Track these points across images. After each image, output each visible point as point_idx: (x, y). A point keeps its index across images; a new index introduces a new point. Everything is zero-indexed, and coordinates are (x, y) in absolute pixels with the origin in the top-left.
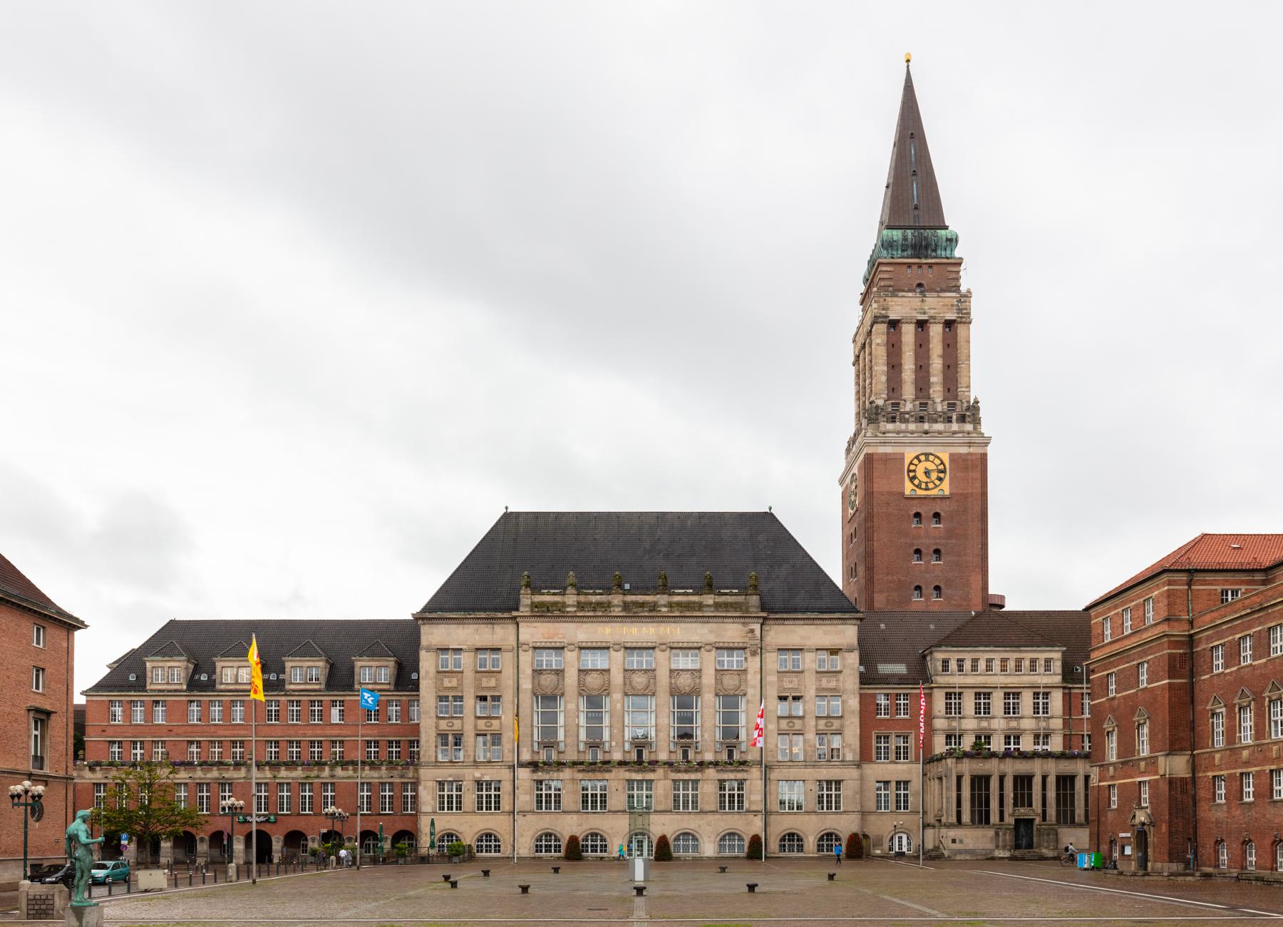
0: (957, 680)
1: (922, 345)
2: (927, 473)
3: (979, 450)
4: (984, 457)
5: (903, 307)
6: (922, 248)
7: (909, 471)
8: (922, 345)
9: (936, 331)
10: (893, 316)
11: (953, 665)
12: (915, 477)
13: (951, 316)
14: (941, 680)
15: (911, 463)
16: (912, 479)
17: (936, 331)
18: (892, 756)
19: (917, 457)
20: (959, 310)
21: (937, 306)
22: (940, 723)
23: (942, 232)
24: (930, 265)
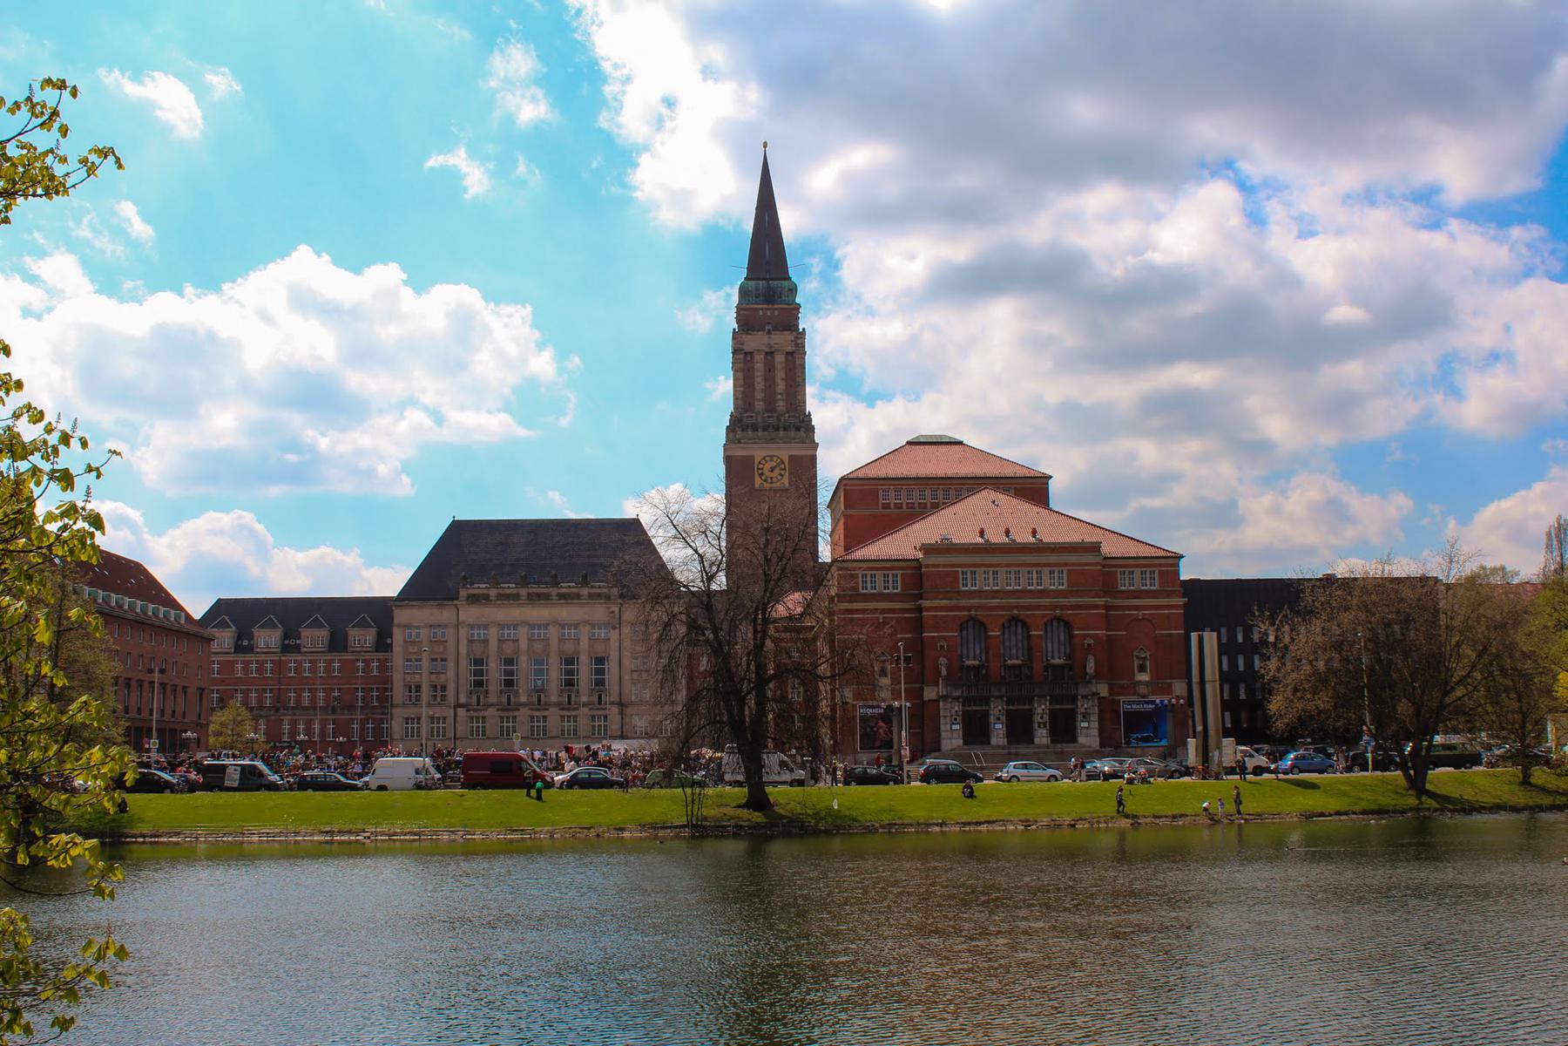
1: (770, 369)
2: (772, 470)
3: (810, 453)
5: (756, 341)
6: (770, 297)
8: (770, 369)
9: (780, 359)
10: (747, 348)
13: (789, 349)
16: (761, 475)
17: (780, 359)
20: (797, 345)
21: (781, 340)
23: (785, 283)
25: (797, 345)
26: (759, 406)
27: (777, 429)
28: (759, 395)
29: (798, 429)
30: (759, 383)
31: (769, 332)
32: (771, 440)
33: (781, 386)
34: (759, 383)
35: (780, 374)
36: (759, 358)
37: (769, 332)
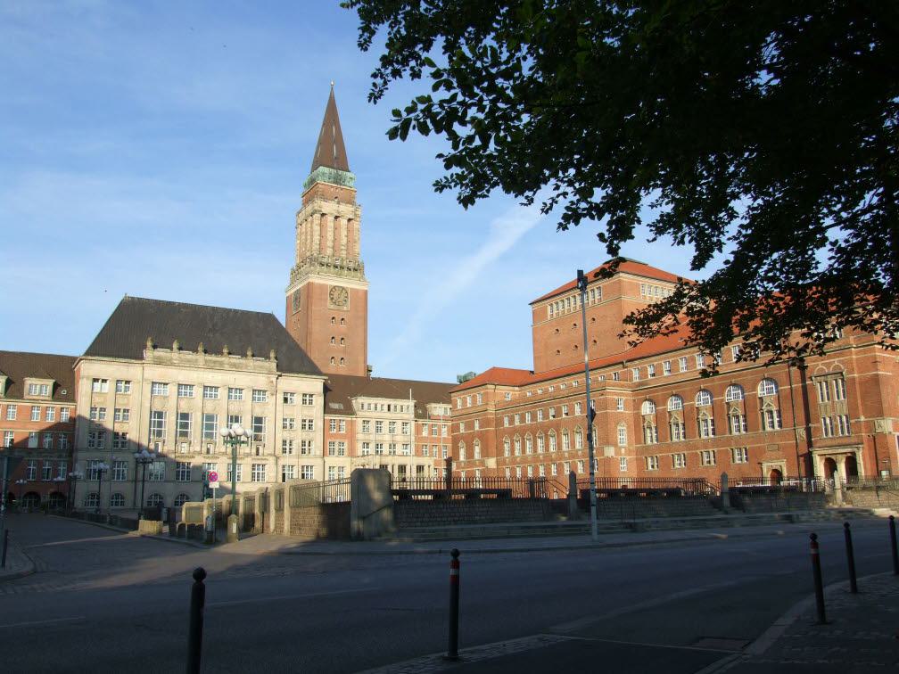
0: (368, 414)
4: (366, 292)
7: (331, 294)
9: (344, 222)
11: (366, 407)
12: (332, 299)
13: (351, 217)
14: (360, 413)
15: (332, 290)
17: (344, 222)
18: (336, 453)
19: (334, 287)
20: (355, 215)
21: (346, 210)
22: (360, 436)
24: (342, 189)
25: (355, 215)
26: (329, 251)
27: (342, 268)
28: (330, 244)
29: (355, 270)
30: (330, 235)
31: (338, 203)
32: (340, 275)
33: (344, 241)
34: (330, 235)
35: (344, 233)
36: (330, 219)
37: (338, 203)
